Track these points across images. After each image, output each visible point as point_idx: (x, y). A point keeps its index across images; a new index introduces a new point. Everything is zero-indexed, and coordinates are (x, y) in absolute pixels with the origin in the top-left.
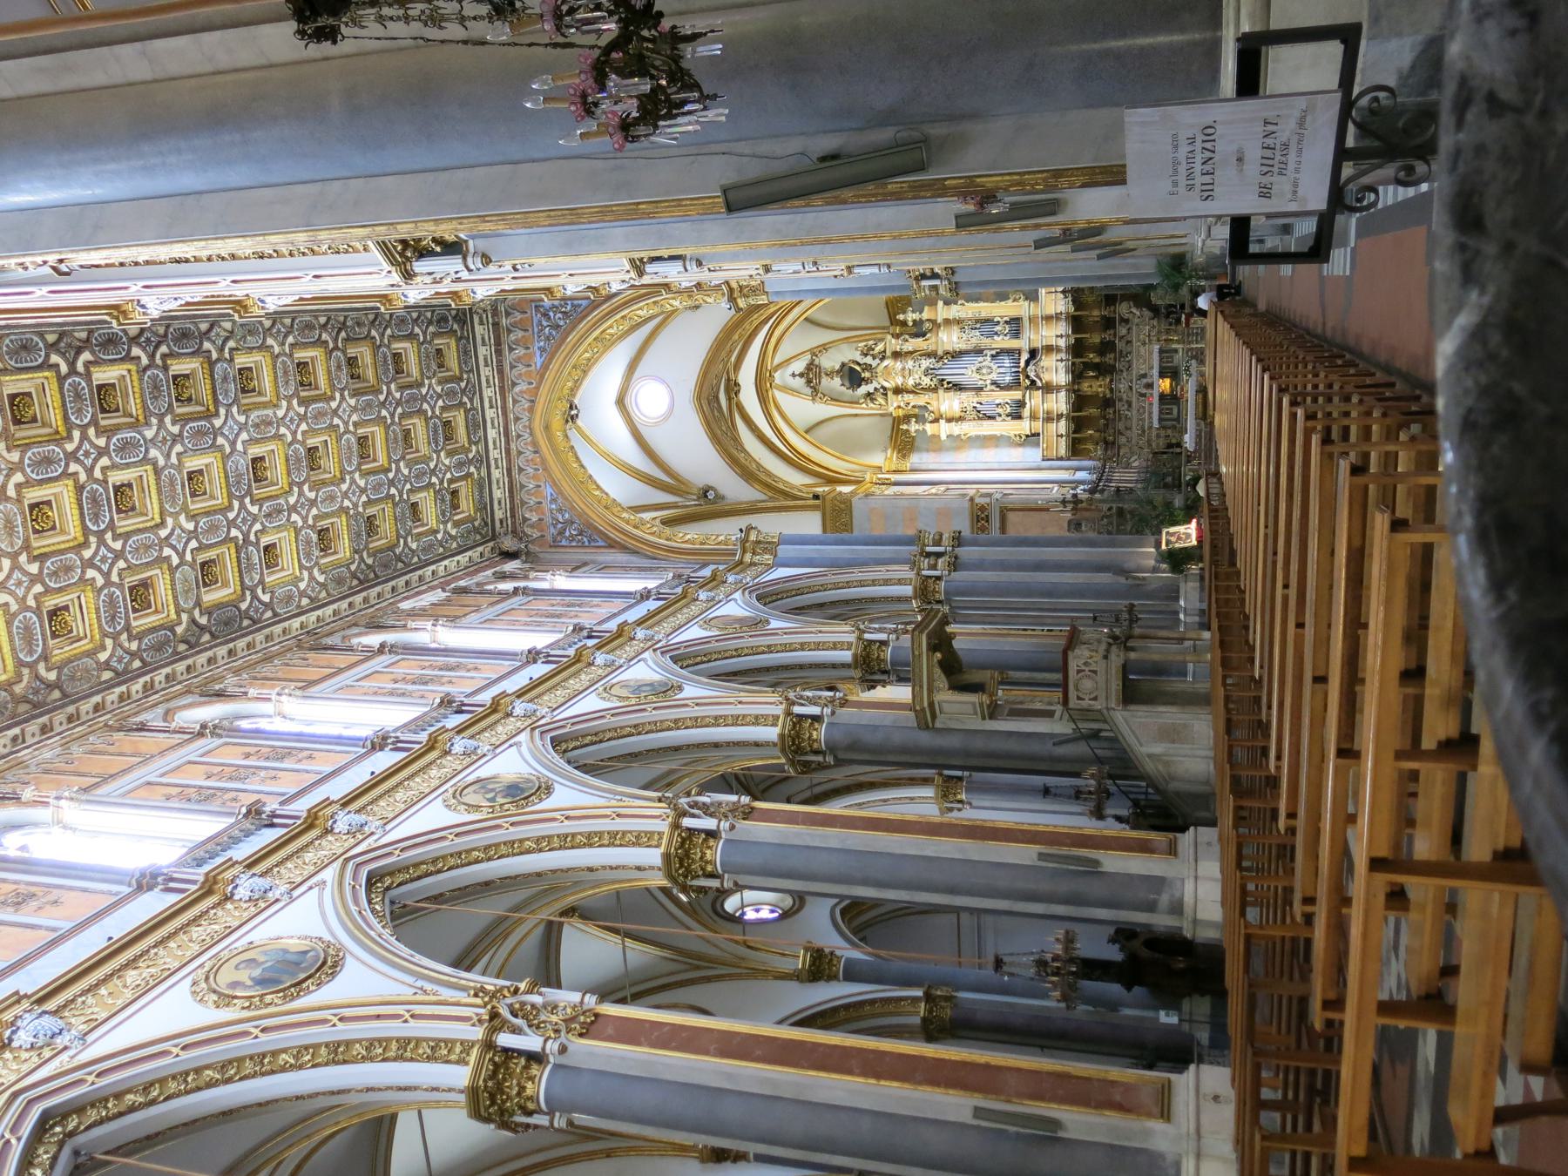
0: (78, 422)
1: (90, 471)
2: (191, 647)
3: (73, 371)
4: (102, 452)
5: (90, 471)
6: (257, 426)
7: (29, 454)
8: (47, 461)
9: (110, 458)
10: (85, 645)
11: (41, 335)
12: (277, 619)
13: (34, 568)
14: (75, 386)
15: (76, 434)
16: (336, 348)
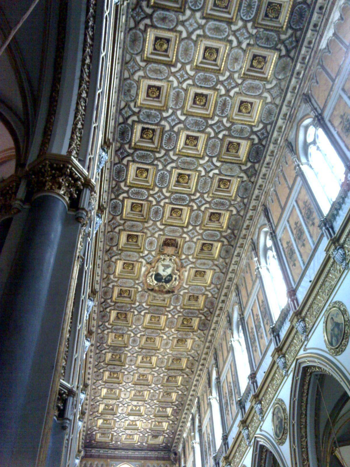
0: (146, 197)
1: (166, 198)
2: (255, 174)
3: (127, 192)
4: (161, 191)
5: (166, 198)
6: (176, 104)
7: (152, 218)
8: (156, 212)
9: (164, 188)
10: (227, 215)
11: (112, 200)
12: (274, 124)
13: (190, 227)
14: (133, 193)
15: (151, 199)
16: (150, 16)
